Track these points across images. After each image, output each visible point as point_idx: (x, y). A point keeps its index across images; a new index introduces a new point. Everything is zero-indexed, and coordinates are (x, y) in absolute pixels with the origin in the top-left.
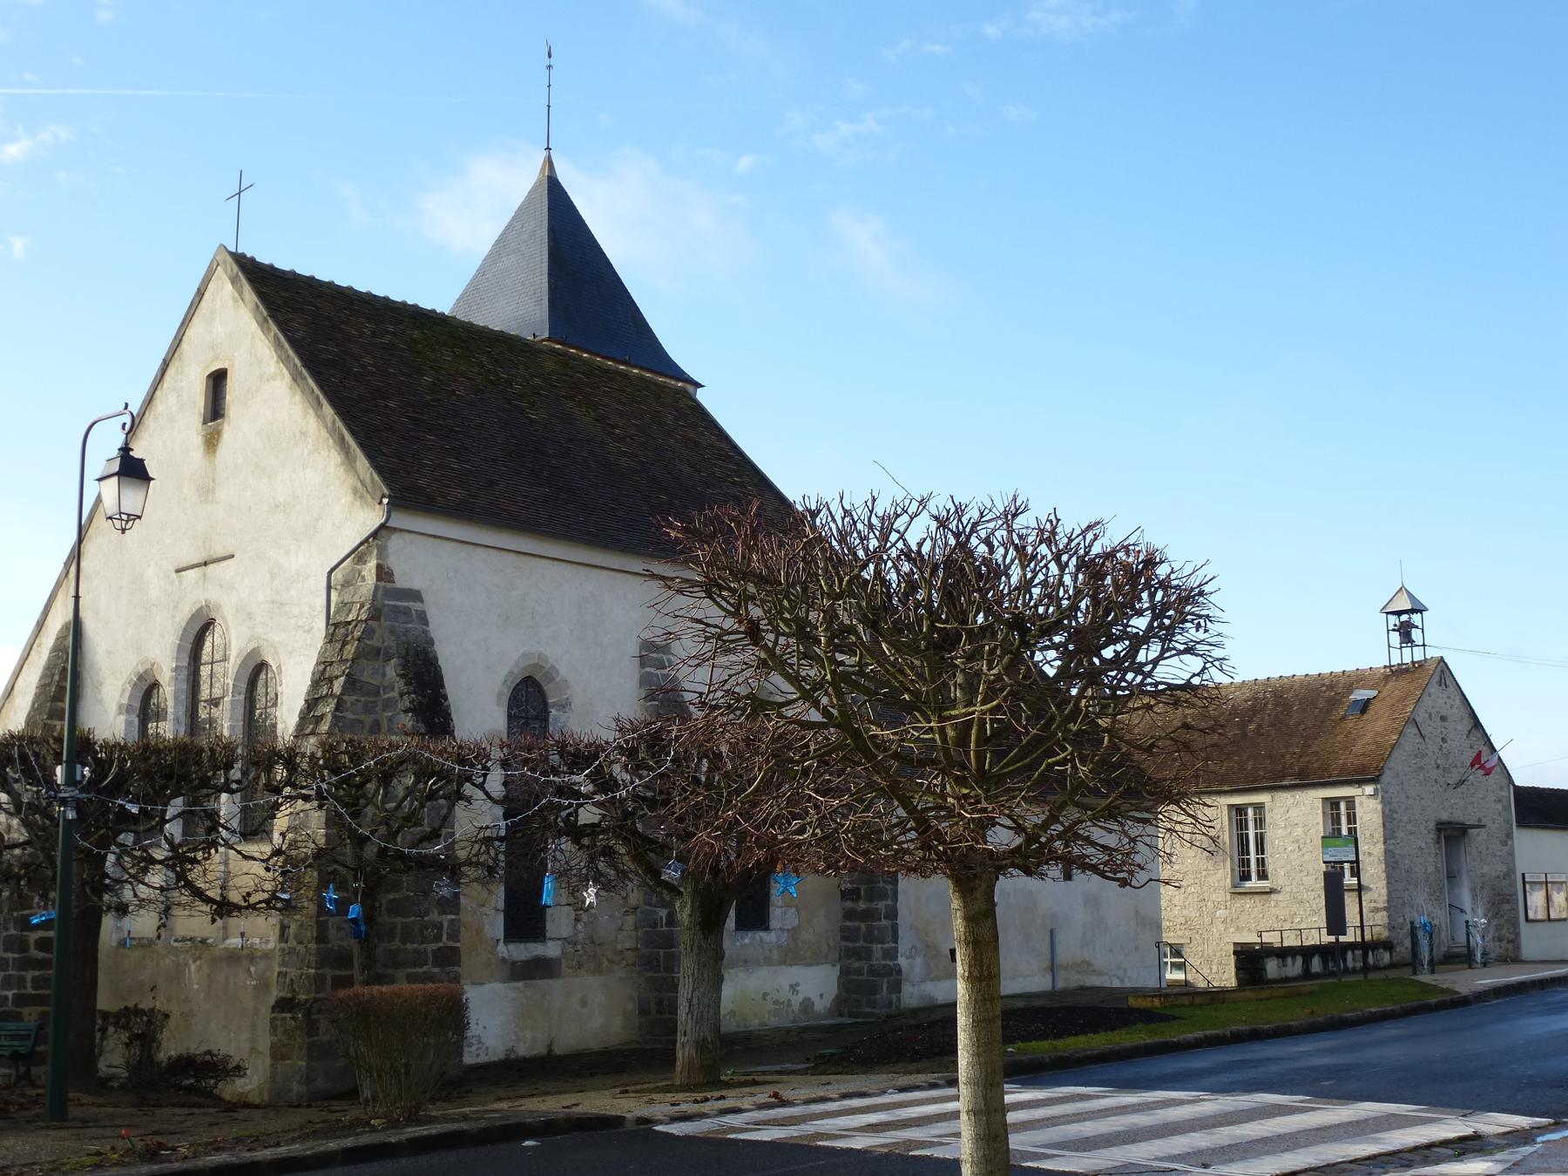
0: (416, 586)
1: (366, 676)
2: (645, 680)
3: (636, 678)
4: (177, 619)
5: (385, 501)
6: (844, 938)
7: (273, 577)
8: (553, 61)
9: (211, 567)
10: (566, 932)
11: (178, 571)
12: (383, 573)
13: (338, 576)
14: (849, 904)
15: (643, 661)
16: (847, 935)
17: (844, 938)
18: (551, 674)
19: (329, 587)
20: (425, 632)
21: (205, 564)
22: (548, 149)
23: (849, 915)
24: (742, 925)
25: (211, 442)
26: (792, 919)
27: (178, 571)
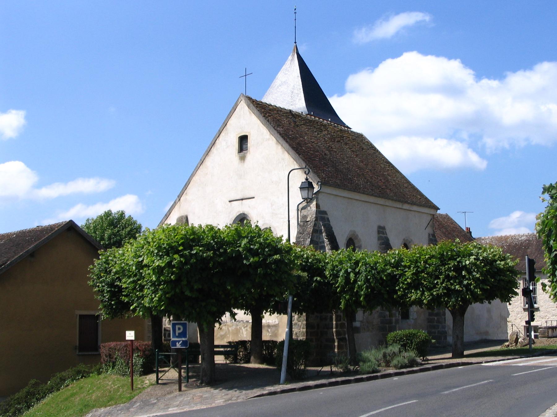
0: (325, 210)
1: (315, 239)
2: (379, 239)
3: (377, 238)
4: (231, 217)
5: (319, 184)
6: (428, 322)
7: (272, 205)
8: (296, 11)
9: (244, 201)
10: (361, 319)
11: (230, 201)
12: (318, 206)
13: (301, 206)
14: (430, 311)
15: (379, 232)
16: (430, 321)
17: (428, 322)
18: (357, 237)
19: (298, 210)
20: (330, 225)
21: (242, 200)
22: (295, 43)
23: (430, 314)
24: (429, 313)
25: (243, 159)
26: (415, 316)
27: (230, 201)
